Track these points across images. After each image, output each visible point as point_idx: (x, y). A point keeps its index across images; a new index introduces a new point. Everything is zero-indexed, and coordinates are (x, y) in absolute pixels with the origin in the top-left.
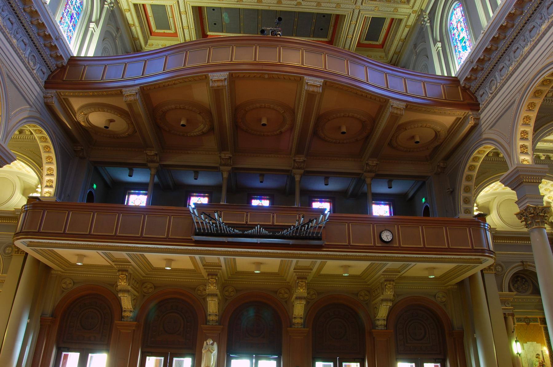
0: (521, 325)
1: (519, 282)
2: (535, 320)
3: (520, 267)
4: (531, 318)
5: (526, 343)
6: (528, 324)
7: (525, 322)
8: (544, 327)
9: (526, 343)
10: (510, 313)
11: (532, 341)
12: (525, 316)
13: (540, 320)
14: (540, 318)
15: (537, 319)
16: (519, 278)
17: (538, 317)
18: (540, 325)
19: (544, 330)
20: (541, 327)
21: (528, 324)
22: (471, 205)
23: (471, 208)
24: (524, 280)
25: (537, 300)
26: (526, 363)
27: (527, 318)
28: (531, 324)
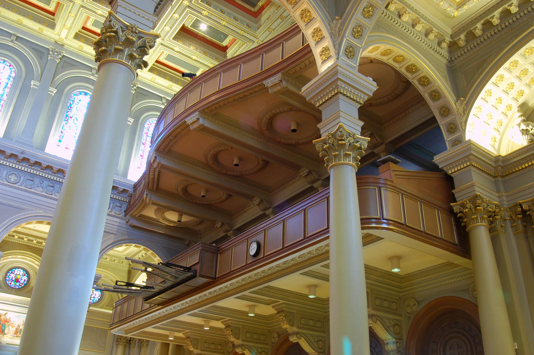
22: (460, 132)
23: (461, 135)
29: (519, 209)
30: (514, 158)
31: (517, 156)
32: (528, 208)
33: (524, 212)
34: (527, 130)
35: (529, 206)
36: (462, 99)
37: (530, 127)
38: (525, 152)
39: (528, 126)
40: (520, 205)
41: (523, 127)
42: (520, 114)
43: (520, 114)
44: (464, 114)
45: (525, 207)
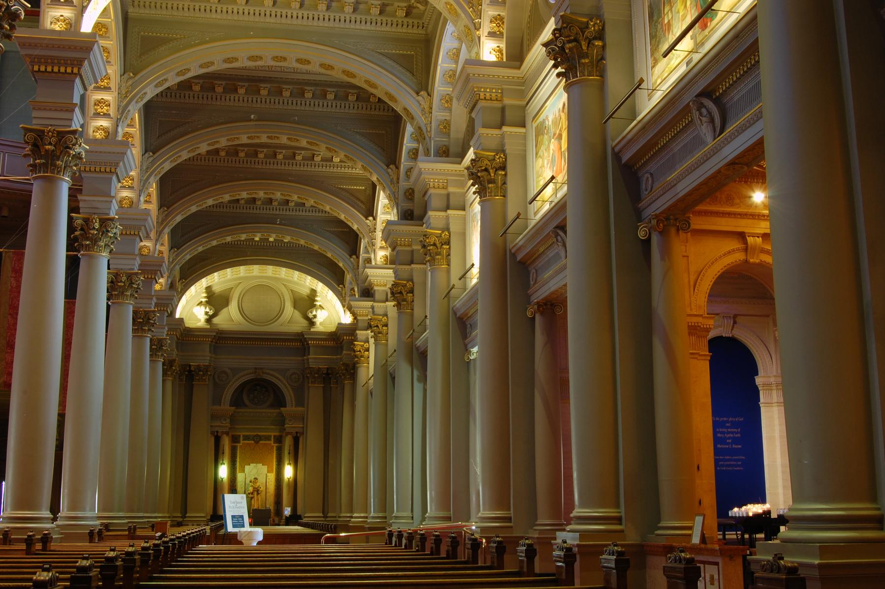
0: (248, 443)
1: (256, 392)
2: (268, 438)
3: (252, 375)
4: (263, 436)
5: (250, 465)
6: (257, 442)
7: (254, 440)
8: (276, 447)
9: (250, 465)
10: (224, 431)
11: (257, 463)
12: (255, 434)
13: (274, 439)
14: (274, 436)
15: (271, 436)
16: (258, 387)
17: (272, 434)
18: (273, 444)
19: (276, 450)
20: (273, 446)
21: (257, 442)
24: (264, 389)
25: (275, 414)
26: (242, 488)
27: (257, 435)
28: (261, 443)
29: (188, 368)
30: (196, 332)
31: (201, 332)
32: (193, 370)
33: (190, 371)
34: (208, 312)
35: (195, 369)
36: (184, 280)
37: (212, 311)
38: (203, 332)
39: (211, 310)
40: (190, 365)
41: (208, 310)
42: (205, 295)
43: (205, 295)
44: (181, 292)
45: (192, 369)
